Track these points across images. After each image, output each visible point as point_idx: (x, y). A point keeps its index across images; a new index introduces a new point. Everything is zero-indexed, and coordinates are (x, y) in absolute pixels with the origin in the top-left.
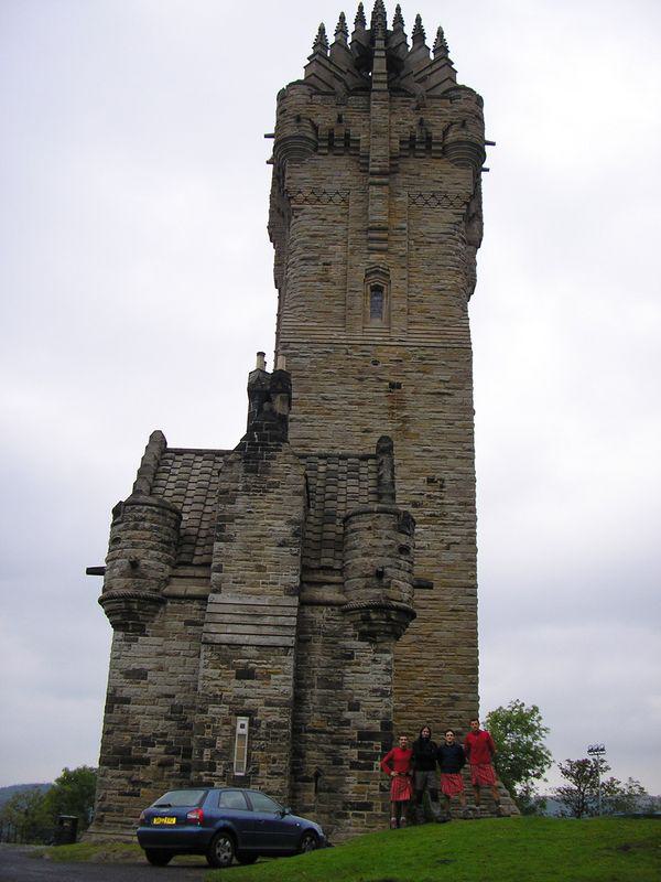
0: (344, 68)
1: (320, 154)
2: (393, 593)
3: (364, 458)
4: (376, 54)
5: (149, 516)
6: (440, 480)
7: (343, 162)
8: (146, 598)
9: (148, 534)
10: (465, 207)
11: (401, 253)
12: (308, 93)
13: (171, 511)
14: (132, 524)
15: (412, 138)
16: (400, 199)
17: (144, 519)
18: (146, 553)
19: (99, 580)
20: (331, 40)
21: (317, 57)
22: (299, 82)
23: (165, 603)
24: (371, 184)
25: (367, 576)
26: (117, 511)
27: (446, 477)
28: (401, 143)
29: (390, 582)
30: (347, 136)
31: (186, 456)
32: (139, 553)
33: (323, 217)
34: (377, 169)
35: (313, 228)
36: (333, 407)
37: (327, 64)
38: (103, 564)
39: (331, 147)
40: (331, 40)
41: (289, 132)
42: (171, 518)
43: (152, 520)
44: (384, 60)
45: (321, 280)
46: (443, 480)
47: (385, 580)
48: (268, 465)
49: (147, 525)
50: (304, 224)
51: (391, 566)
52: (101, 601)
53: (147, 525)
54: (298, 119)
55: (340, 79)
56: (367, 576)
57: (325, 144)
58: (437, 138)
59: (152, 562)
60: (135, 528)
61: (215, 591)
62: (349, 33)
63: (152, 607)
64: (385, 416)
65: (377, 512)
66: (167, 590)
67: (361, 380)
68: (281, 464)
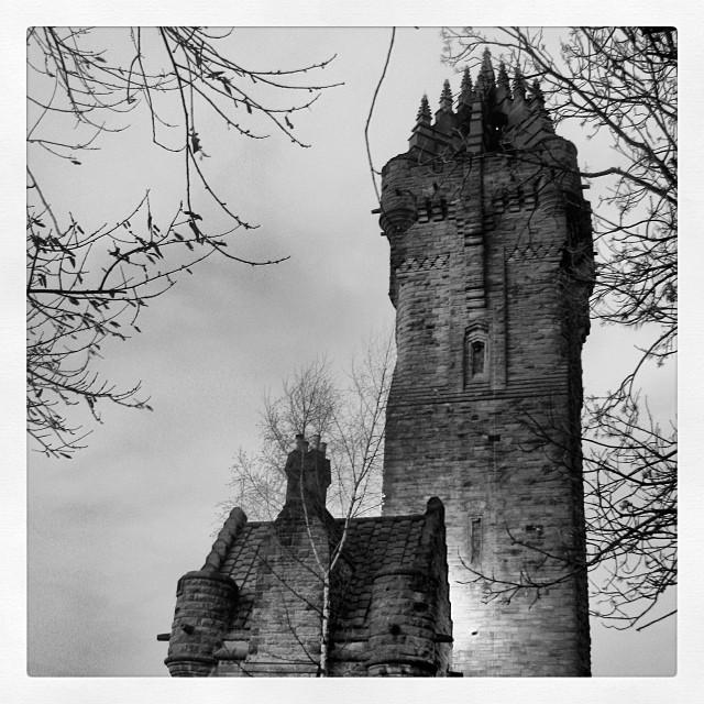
0: (449, 134)
1: (421, 223)
2: (408, 648)
3: (416, 519)
4: (473, 117)
5: (203, 588)
6: (539, 526)
7: (442, 225)
8: (197, 660)
9: (201, 604)
10: (561, 254)
11: (499, 308)
12: (407, 166)
13: (222, 581)
14: (188, 596)
15: (505, 195)
16: (496, 255)
17: (197, 591)
18: (199, 621)
19: (166, 644)
20: (435, 107)
21: (418, 129)
22: (400, 157)
23: (217, 664)
24: (467, 245)
25: (384, 633)
26: (181, 584)
27: (542, 523)
28: (494, 201)
29: (405, 638)
30: (444, 202)
31: (261, 528)
32: (191, 622)
33: (425, 282)
34: (471, 231)
35: (417, 294)
36: (436, 464)
37: (429, 133)
38: (170, 631)
39: (430, 215)
40: (435, 107)
41: (390, 205)
42: (223, 589)
43: (204, 592)
44: (480, 122)
45: (426, 343)
46: (541, 527)
47: (399, 637)
48: (300, 537)
49: (201, 595)
50: (405, 291)
51: (406, 623)
52: (166, 663)
53: (201, 595)
54: (398, 193)
55: (446, 145)
56: (384, 633)
57: (424, 213)
58: (528, 191)
59: (205, 628)
60: (192, 599)
61: (251, 653)
62: (455, 99)
63: (203, 668)
64: (487, 468)
65: (395, 574)
66: (217, 652)
67: (461, 436)
68: (313, 540)
